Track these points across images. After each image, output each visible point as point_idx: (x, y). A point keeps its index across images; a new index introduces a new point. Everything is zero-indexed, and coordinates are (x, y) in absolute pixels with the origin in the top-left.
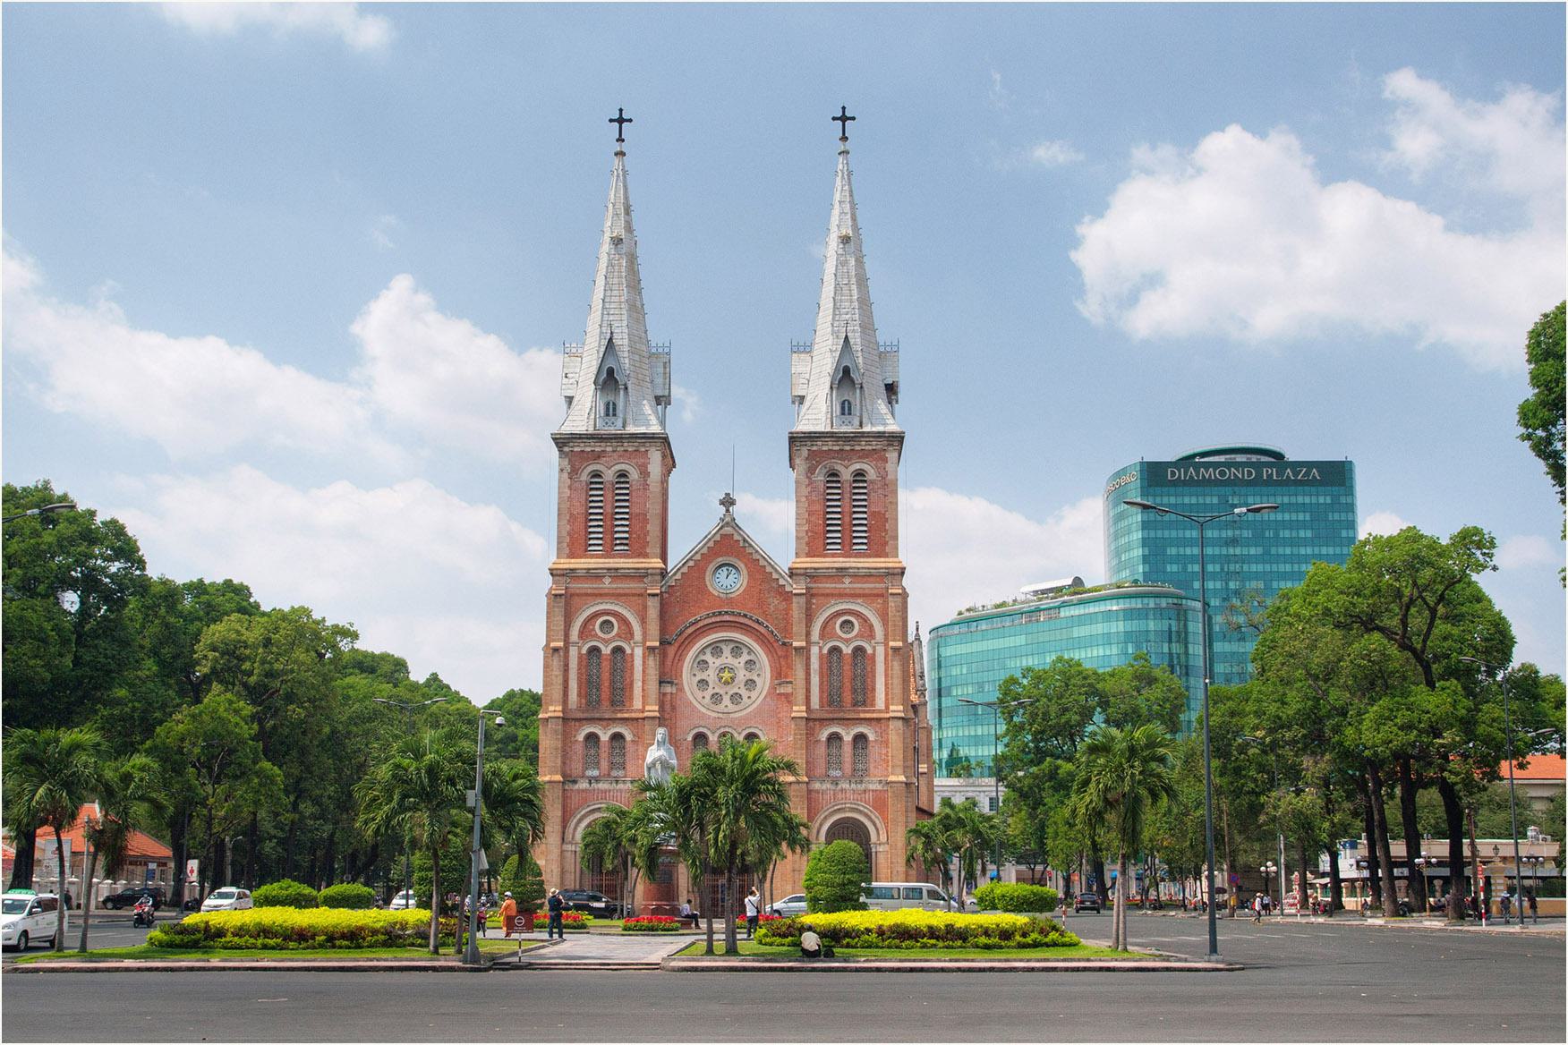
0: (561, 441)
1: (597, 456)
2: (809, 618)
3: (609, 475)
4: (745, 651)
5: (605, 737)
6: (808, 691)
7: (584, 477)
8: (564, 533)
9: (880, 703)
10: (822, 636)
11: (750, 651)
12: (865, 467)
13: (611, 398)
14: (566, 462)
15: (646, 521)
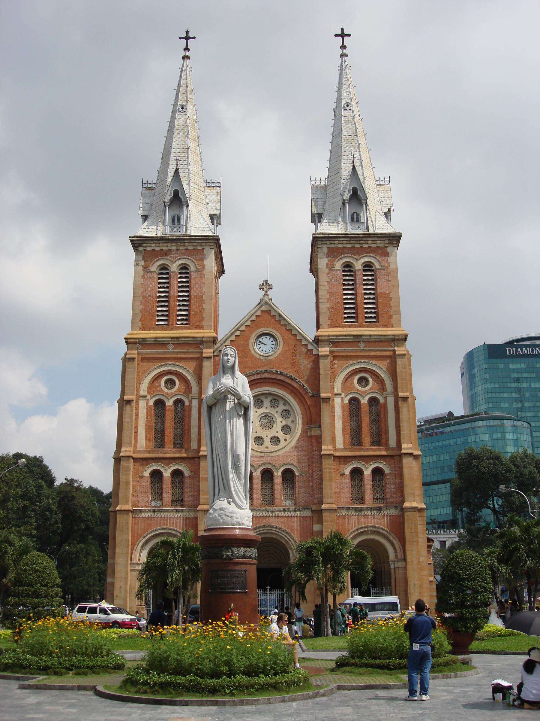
0: (137, 243)
1: (165, 254)
2: (334, 376)
3: (174, 267)
4: (281, 403)
5: (167, 473)
6: (334, 433)
7: (154, 268)
8: (138, 311)
9: (393, 443)
10: (343, 389)
11: (286, 402)
12: (372, 260)
13: (176, 212)
14: (141, 258)
15: (202, 301)
